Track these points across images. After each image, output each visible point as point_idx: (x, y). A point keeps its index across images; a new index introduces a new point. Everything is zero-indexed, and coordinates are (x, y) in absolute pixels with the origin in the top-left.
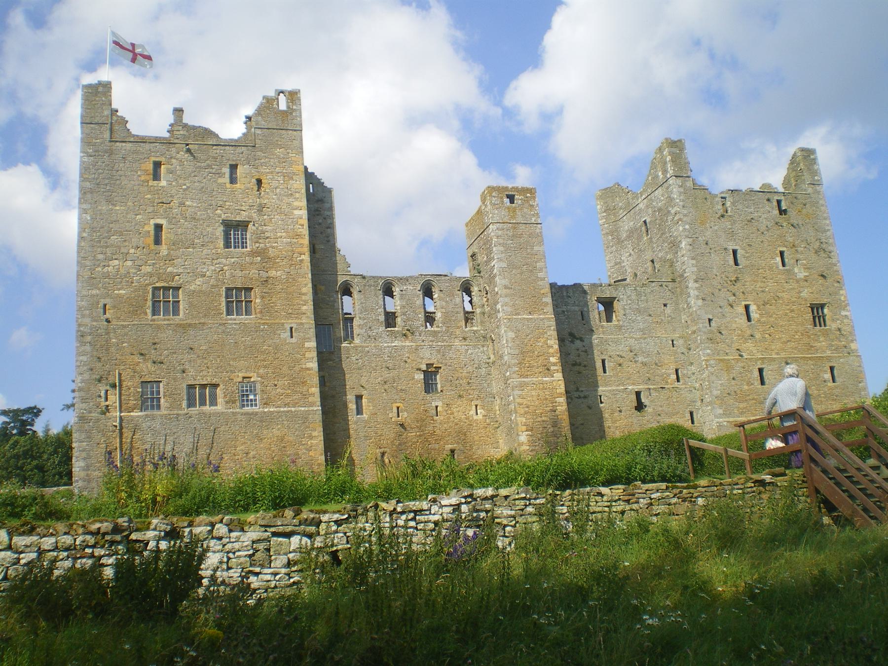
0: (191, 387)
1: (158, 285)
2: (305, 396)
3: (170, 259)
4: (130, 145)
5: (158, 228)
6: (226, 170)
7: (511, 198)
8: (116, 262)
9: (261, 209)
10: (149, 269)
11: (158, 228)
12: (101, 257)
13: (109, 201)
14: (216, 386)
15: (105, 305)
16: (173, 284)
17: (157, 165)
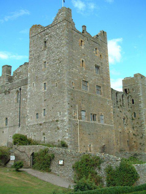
0: (91, 114)
1: (83, 79)
2: (112, 121)
3: (86, 72)
4: (76, 32)
5: (83, 61)
6: (95, 49)
7: (142, 77)
8: (74, 69)
9: (102, 63)
10: (81, 74)
11: (83, 61)
12: (71, 66)
13: (72, 48)
14: (96, 115)
15: (73, 82)
16: (86, 81)
17: (82, 41)
